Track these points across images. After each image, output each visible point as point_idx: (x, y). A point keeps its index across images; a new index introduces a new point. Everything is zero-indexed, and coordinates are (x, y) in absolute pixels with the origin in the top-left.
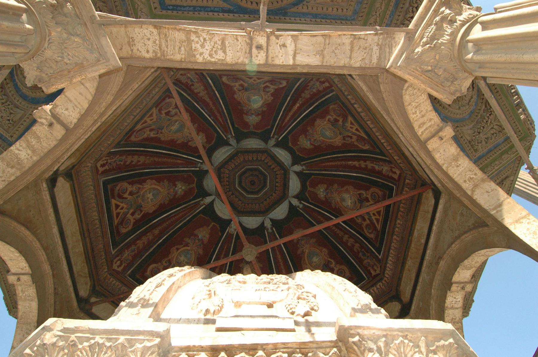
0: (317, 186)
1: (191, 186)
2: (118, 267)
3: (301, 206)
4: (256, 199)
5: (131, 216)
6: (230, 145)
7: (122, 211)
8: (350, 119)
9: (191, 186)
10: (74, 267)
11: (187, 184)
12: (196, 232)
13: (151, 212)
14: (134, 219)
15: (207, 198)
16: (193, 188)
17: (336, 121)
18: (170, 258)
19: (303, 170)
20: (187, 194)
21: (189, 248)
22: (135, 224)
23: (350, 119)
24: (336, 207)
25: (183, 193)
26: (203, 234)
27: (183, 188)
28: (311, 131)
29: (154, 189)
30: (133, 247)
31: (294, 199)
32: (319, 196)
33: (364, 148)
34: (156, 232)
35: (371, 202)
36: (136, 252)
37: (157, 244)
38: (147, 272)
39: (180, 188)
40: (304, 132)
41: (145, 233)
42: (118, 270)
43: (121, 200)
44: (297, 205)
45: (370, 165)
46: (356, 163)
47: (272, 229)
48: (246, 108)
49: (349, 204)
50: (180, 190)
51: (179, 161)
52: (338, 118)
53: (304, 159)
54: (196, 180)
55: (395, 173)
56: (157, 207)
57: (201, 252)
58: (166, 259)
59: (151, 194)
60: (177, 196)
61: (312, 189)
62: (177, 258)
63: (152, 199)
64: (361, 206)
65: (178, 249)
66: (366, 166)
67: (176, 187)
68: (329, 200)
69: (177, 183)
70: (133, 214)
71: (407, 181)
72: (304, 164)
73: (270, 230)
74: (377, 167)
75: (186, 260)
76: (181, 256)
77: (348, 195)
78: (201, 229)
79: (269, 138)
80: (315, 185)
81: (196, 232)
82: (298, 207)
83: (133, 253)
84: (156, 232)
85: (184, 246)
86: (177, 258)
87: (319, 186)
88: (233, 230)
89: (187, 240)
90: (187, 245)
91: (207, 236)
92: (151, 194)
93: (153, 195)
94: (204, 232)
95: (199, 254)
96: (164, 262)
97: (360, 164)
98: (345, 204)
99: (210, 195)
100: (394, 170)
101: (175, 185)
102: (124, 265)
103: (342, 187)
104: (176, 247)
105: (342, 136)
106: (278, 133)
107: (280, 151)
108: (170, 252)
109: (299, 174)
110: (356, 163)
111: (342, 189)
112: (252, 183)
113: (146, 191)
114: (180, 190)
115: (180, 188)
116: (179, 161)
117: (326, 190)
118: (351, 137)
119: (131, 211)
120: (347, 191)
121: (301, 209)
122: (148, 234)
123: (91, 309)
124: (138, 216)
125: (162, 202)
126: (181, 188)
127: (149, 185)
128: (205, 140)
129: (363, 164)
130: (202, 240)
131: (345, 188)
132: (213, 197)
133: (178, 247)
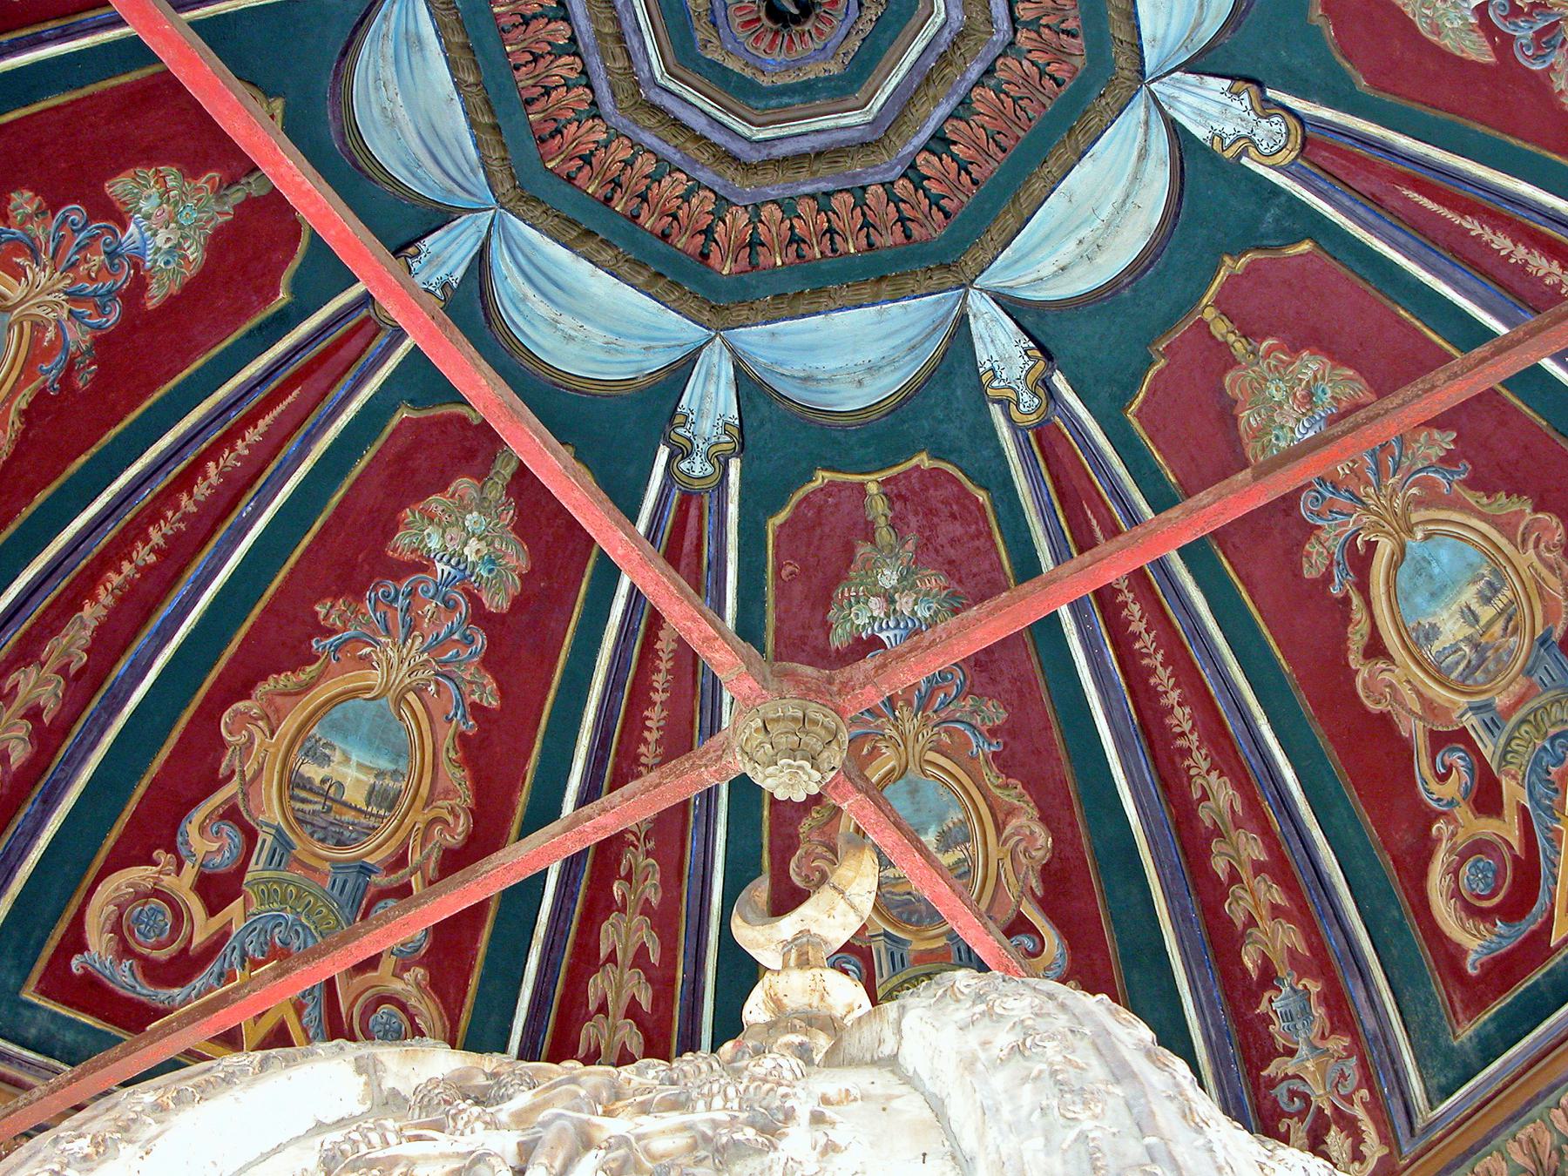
1: (879, 508)
6: (481, 260)
9: (879, 508)
11: (863, 549)
16: (895, 494)
18: (1414, 729)
21: (1385, 547)
36: (1315, 988)
38: (1462, 952)
41: (1204, 891)
50: (904, 604)
56: (1013, 795)
58: (1422, 766)
65: (1375, 649)
75: (1469, 595)
78: (1248, 418)
83: (1319, 1012)
84: (1220, 797)
85: (1363, 587)
86: (1439, 674)
89: (1315, 559)
90: (1360, 561)
91: (1311, 365)
94: (1276, 391)
95: (1448, 460)
102: (1359, 1112)
104: (1355, 659)
108: (1385, 720)
122: (1219, 865)
125: (983, 748)
128: (463, 485)
132: (982, 309)
133: (1357, 638)
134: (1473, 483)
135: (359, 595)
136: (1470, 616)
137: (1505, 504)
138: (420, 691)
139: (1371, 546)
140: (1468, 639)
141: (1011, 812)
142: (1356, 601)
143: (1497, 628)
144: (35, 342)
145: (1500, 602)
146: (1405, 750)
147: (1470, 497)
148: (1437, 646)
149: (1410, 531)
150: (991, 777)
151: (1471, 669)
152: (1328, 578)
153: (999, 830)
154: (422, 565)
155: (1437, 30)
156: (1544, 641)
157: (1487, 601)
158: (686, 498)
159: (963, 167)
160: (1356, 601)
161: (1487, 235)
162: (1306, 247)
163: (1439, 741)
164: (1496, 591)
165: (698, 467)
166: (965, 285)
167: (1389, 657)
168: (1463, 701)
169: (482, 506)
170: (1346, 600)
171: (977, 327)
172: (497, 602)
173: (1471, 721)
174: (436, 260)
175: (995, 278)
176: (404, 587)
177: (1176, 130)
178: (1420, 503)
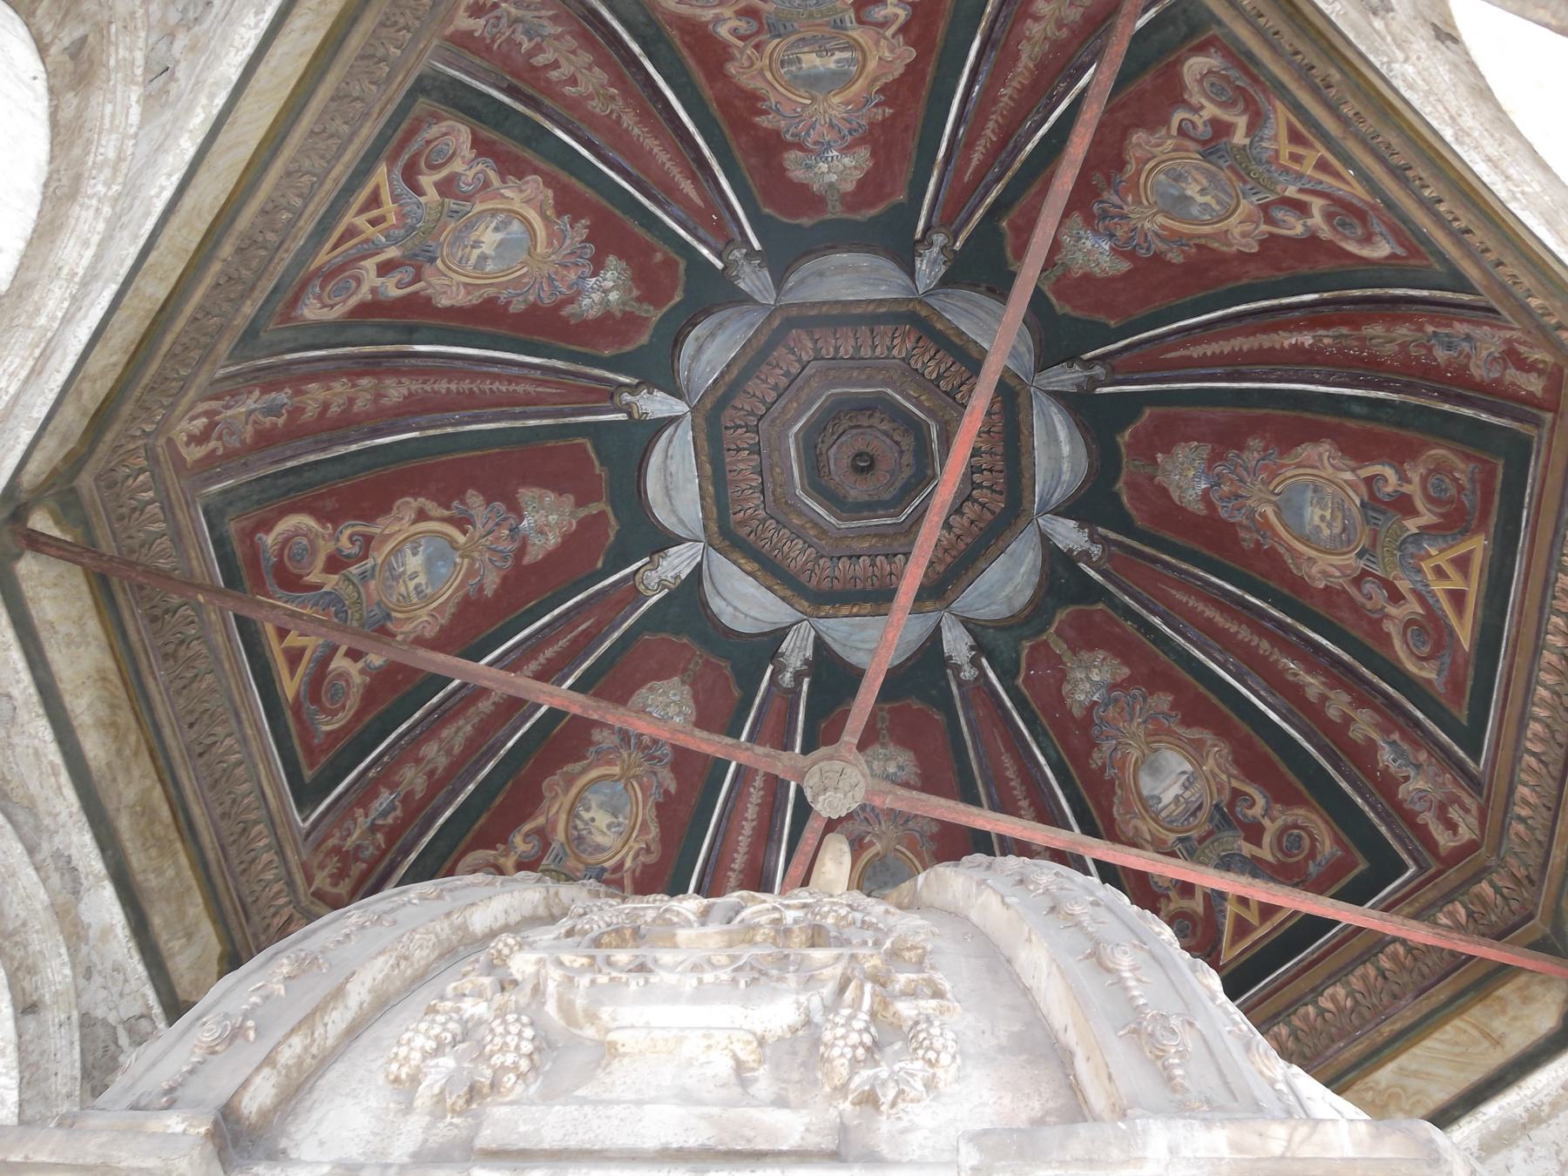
0: (1091, 647)
3: (968, 673)
4: (823, 531)
5: (373, 272)
6: (911, 272)
7: (370, 230)
8: (1478, 546)
12: (526, 494)
13: (444, 302)
15: (659, 394)
17: (1403, 505)
19: (1086, 555)
20: (609, 325)
22: (364, 310)
23: (1478, 546)
24: (1103, 769)
25: (593, 314)
26: (546, 519)
27: (614, 296)
28: (1252, 457)
29: (526, 221)
31: (960, 630)
32: (1066, 688)
33: (1411, 667)
34: (396, 391)
35: (1266, 853)
36: (281, 421)
37: (368, 443)
38: (268, 531)
39: (605, 290)
40: (1226, 440)
42: (183, 451)
43: (402, 187)
44: (957, 660)
45: (1364, 725)
46: (1313, 685)
47: (798, 677)
48: (1115, 199)
49: (1168, 798)
51: (687, 187)
52: (1419, 504)
53: (1123, 523)
54: (677, 299)
55: (1452, 826)
56: (475, 299)
57: (491, 582)
59: (499, 236)
60: (565, 312)
61: (1059, 648)
62: (397, 551)
63: (483, 258)
64: (1210, 834)
65: (422, 516)
66: (1348, 720)
67: (595, 274)
68: (1095, 731)
69: (612, 260)
70: (385, 269)
71: (1484, 885)
72: (1105, 541)
73: (787, 678)
74: (1386, 756)
75: (422, 579)
76: (414, 554)
77: (1188, 767)
78: (550, 497)
79: (1071, 358)
80: (1087, 638)
81: (526, 494)
82: (957, 669)
83: (268, 421)
84: (396, 391)
86: (397, 551)
87: (1101, 654)
88: (653, 584)
89: (474, 499)
90: (461, 523)
91: (553, 540)
92: (499, 236)
93: (501, 243)
94: (553, 518)
95: (481, 589)
96: (348, 532)
97: (1324, 698)
98: (1147, 785)
99: (676, 392)
100: (1454, 813)
101: (598, 266)
102: (212, 444)
103: (1188, 722)
105: (1361, 563)
106: (1117, 368)
107: (1062, 434)
109: (1056, 561)
110: (1313, 685)
111: (1181, 730)
112: (864, 465)
113: (494, 213)
114: (596, 297)
115: (605, 290)
116: (687, 187)
117: (1113, 687)
118: (1396, 597)
119: (392, 253)
120: (1195, 751)
121: (961, 684)
123: (19, 556)
125: (504, 296)
126: (606, 292)
127: (526, 198)
128: (849, 187)
129: (1338, 704)
130: (525, 539)
131: (1195, 733)
132: (680, 407)
134: (467, 596)
135: (871, 124)
136: (414, 575)
137: (451, 609)
138: (805, 106)
139: (465, 532)
140: (404, 573)
141: (468, 293)
142: (447, 513)
143: (403, 590)
144: (1137, 195)
145: (413, 594)
146: (369, 518)
147: (461, 593)
148: (409, 552)
149: (462, 557)
150: (492, 291)
151: (392, 569)
152: (463, 502)
153: (466, 285)
154: (845, 150)
155: (651, 690)
156: (388, 616)
157: (416, 588)
158: (730, 242)
159: (738, 450)
160: (447, 513)
161: (556, 648)
162: (600, 564)
163: (368, 539)
164: (418, 593)
165: (737, 254)
166: (693, 410)
167: (414, 522)
168: (379, 561)
169: (831, 185)
170: (448, 508)
171: (673, 400)
172: (792, 156)
173: (370, 562)
174: (934, 262)
175: (686, 423)
176: (849, 138)
177: (679, 541)
178: (471, 565)
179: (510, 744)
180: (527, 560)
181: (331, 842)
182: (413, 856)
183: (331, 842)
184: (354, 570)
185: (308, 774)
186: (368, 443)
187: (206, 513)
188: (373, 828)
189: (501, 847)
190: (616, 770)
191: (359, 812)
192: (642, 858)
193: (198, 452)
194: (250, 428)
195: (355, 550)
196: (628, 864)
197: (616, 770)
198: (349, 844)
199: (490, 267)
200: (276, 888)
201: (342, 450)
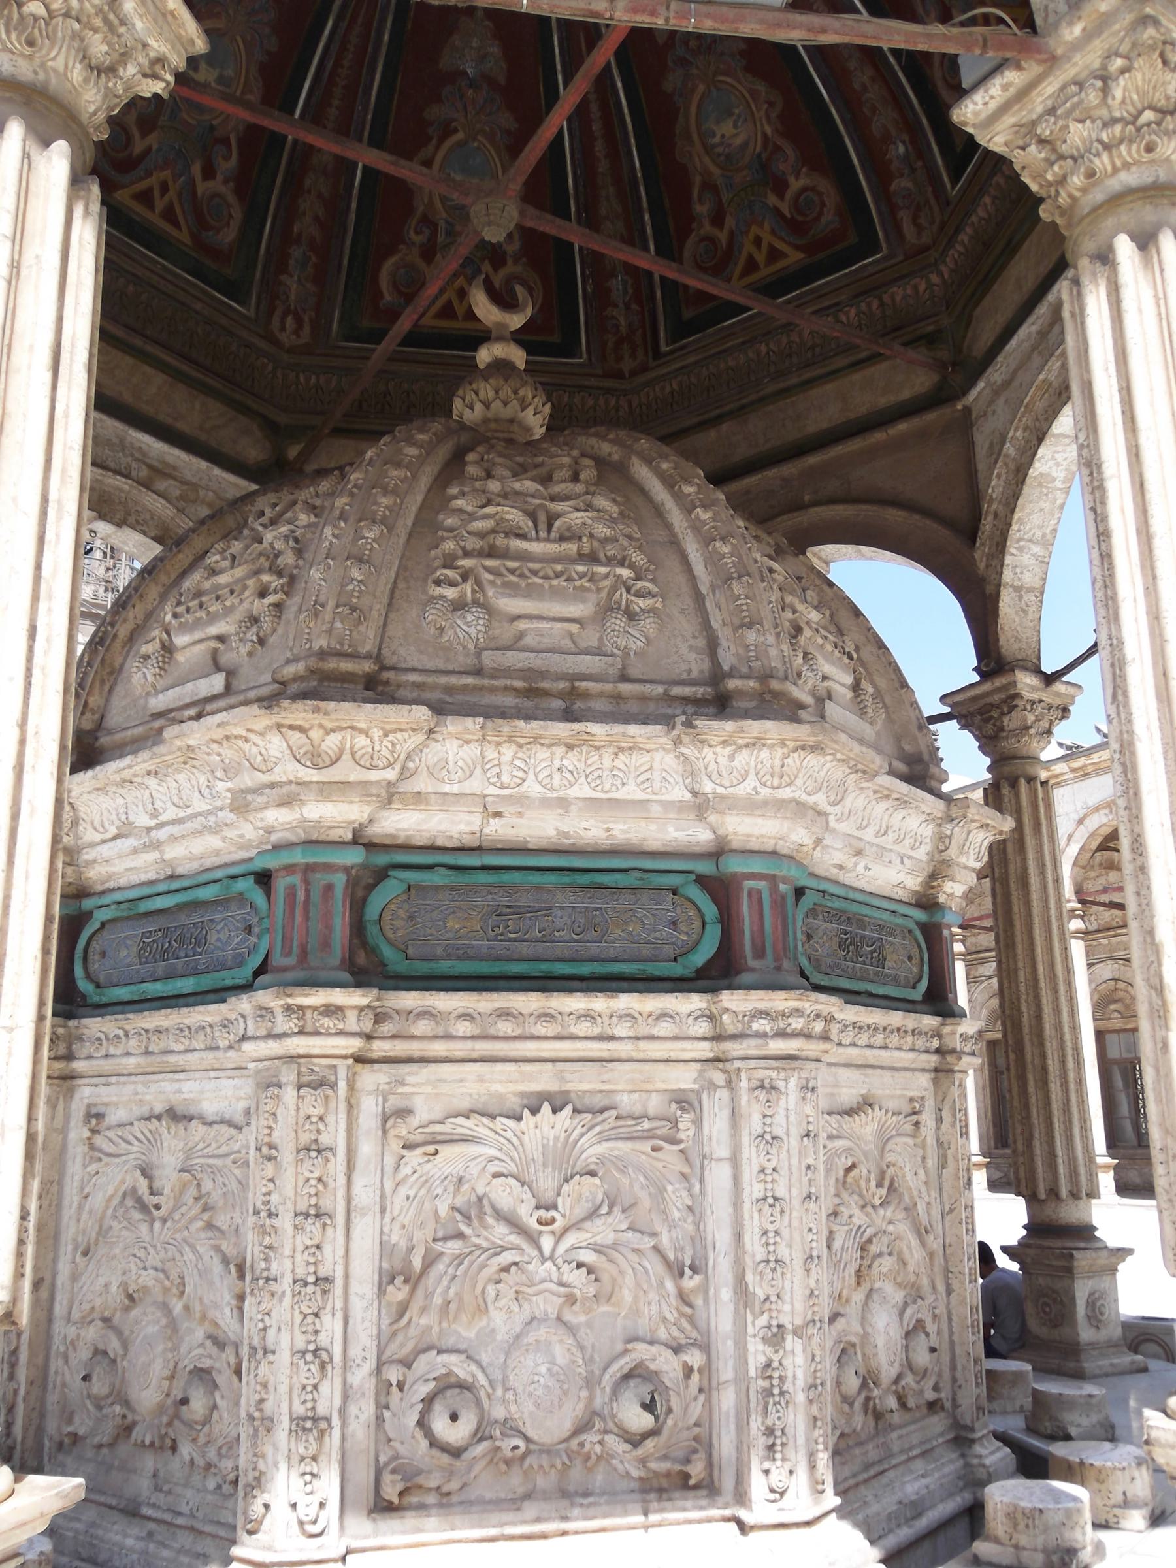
2: (297, 332)
10: (181, 426)
14: (226, 181)
21: (460, 135)
30: (296, 253)
36: (314, 259)
37: (355, 192)
58: (413, 222)
85: (441, 141)
90: (447, 130)
94: (475, 43)
96: (412, 233)
102: (306, 319)
122: (308, 182)
124: (228, 164)
139: (456, 131)
142: (434, 142)
160: (434, 142)
168: (444, 215)
170: (430, 139)
173: (442, 224)
179: (638, 165)
180: (502, 80)
181: (610, 345)
182: (659, 294)
183: (610, 345)
184: (441, 239)
185: (556, 338)
186: (355, 192)
187: (348, 340)
188: (627, 306)
189: (694, 225)
190: (701, 88)
191: (610, 311)
192: (774, 115)
193: (307, 329)
194: (309, 285)
195: (427, 232)
196: (768, 130)
197: (701, 88)
198: (623, 330)
199: (230, 72)
200: (601, 402)
201: (352, 216)
